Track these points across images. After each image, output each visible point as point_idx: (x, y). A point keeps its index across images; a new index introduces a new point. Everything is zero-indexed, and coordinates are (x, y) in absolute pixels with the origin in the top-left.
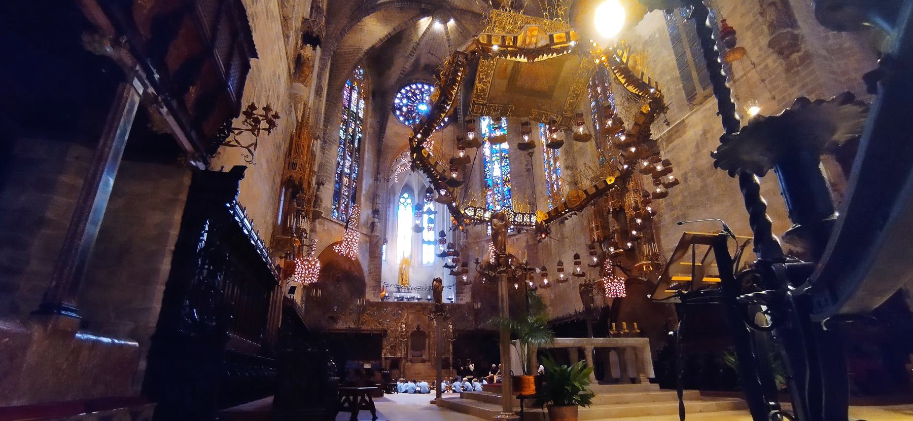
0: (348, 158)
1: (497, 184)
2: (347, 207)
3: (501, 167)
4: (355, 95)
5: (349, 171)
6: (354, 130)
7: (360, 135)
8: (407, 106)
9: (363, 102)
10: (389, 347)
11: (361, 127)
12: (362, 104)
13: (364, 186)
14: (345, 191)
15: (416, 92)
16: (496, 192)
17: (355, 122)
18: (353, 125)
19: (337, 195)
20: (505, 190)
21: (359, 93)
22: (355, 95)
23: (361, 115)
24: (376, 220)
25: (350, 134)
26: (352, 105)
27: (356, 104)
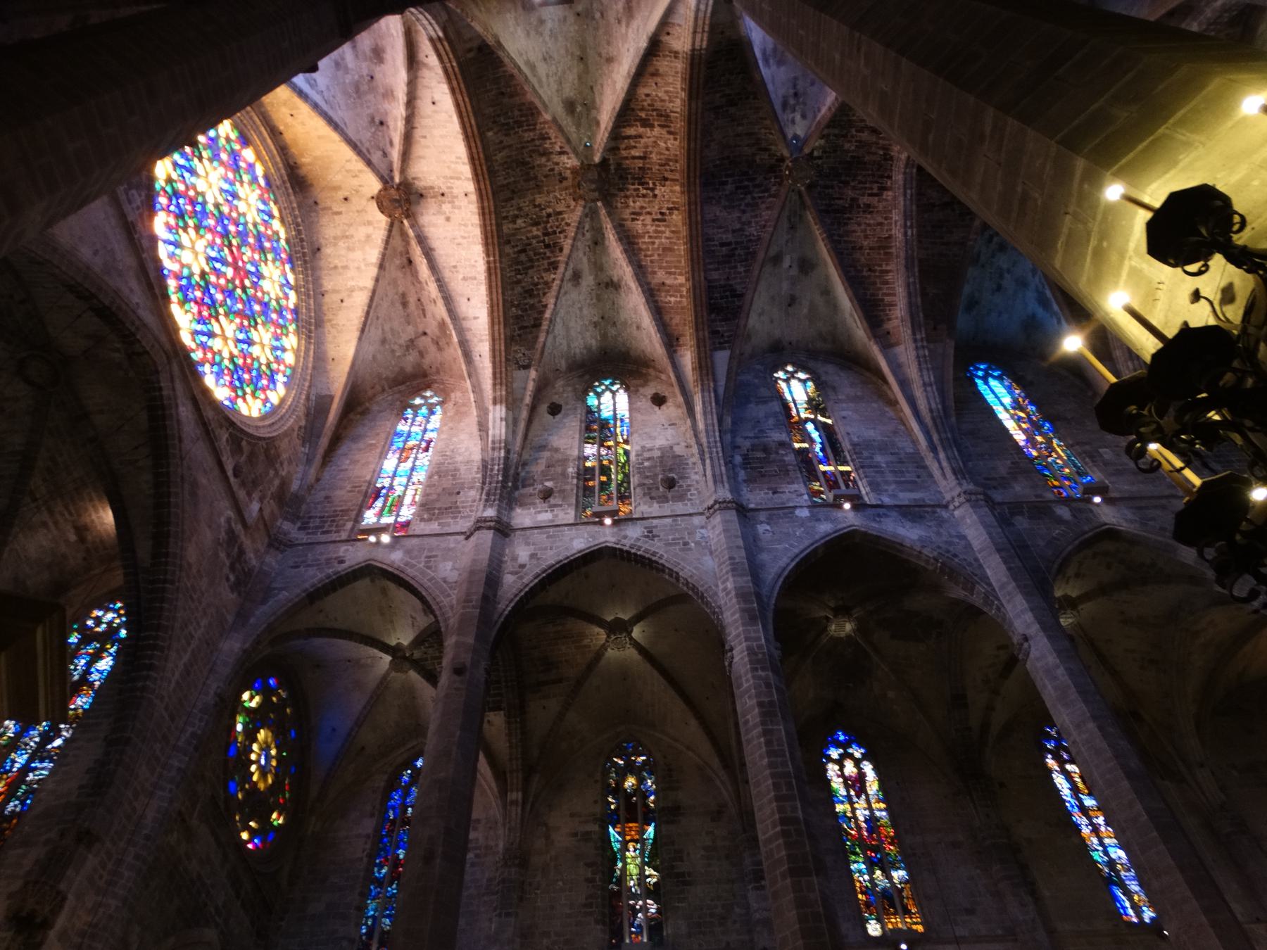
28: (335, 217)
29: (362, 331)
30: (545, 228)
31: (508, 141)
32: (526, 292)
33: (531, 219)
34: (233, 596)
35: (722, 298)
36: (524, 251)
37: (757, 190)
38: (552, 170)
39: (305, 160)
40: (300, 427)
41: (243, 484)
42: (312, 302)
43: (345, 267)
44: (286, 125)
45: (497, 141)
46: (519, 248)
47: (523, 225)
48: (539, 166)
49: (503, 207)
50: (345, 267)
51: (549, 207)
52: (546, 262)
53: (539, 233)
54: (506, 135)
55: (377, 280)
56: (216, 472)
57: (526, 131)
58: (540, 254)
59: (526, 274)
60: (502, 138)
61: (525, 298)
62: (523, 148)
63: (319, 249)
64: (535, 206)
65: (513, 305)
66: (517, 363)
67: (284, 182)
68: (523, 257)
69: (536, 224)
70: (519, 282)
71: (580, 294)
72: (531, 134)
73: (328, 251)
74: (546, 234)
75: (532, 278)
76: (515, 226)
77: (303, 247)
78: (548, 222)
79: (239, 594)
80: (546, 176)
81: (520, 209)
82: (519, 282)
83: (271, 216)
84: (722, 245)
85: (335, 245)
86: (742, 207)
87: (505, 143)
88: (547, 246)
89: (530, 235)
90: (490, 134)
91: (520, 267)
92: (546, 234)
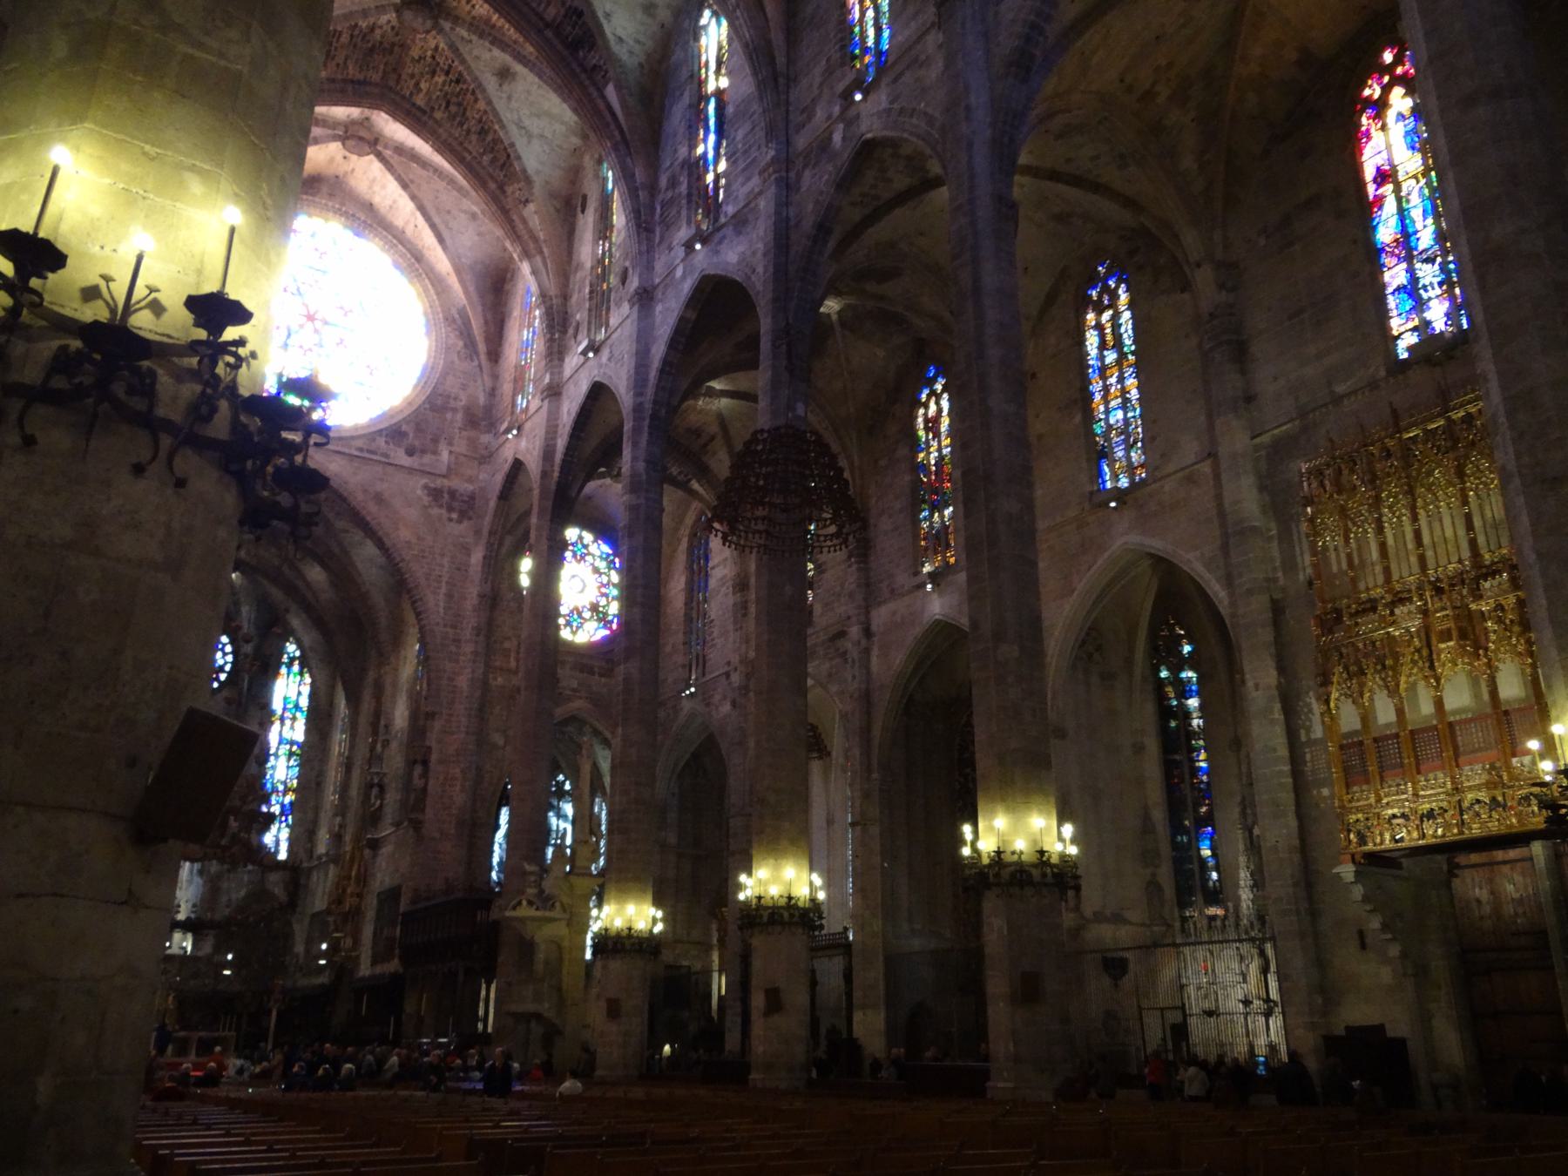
1: (278, 792)
28: (355, 174)
29: (441, 240)
30: (442, 70)
31: (340, 59)
32: (480, 133)
33: (427, 73)
34: (466, 523)
35: (574, 28)
36: (448, 103)
38: (393, 28)
40: (459, 352)
41: (423, 452)
42: (400, 246)
43: (394, 202)
45: (335, 68)
46: (444, 105)
48: (382, 36)
49: (401, 90)
50: (394, 202)
51: (426, 51)
52: (469, 95)
54: (333, 59)
55: (413, 198)
56: (390, 469)
57: (338, 41)
58: (459, 93)
59: (467, 119)
60: (334, 63)
61: (484, 140)
62: (355, 46)
63: (371, 204)
64: (418, 61)
65: (484, 154)
66: (521, 202)
68: (453, 109)
69: (433, 73)
70: (468, 132)
71: (525, 80)
73: (377, 200)
74: (447, 73)
76: (424, 91)
79: (470, 519)
80: (397, 34)
81: (412, 76)
82: (468, 132)
85: (374, 193)
87: (341, 62)
88: (458, 81)
89: (439, 87)
91: (458, 119)
92: (447, 73)
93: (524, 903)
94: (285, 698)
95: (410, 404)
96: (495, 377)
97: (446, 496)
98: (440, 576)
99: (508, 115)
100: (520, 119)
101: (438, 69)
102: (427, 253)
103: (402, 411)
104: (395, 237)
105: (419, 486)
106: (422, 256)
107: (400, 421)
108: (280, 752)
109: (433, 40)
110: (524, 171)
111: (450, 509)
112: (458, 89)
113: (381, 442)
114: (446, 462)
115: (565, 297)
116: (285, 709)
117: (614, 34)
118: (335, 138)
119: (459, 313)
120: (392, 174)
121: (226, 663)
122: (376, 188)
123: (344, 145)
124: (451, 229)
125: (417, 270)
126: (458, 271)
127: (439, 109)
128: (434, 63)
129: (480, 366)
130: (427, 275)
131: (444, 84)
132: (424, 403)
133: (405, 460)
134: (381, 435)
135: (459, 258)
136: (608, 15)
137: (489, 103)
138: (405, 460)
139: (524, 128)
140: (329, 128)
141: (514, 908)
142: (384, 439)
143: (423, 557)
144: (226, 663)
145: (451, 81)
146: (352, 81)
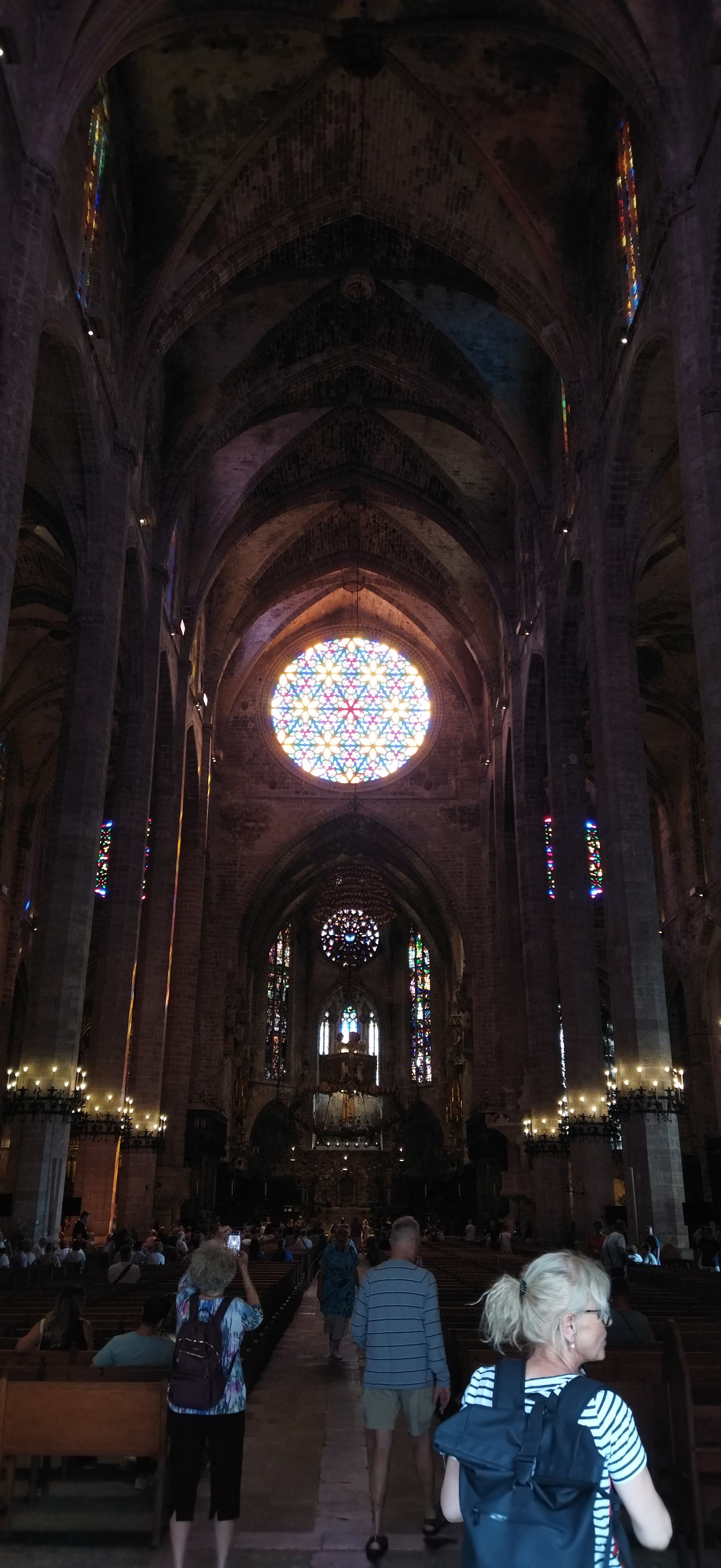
0: (277, 1016)
2: (278, 1065)
3: (424, 1011)
4: (280, 946)
5: (278, 1029)
6: (281, 984)
7: (287, 986)
8: (332, 937)
9: (289, 948)
10: (320, 1193)
11: (288, 977)
12: (288, 953)
13: (293, 1040)
14: (276, 1050)
15: (343, 920)
16: (419, 1037)
17: (282, 974)
18: (280, 979)
19: (269, 1056)
20: (427, 1036)
21: (284, 943)
22: (280, 946)
23: (287, 965)
24: (306, 1072)
25: (277, 991)
26: (278, 959)
27: (281, 956)
29: (424, 629)
33: (374, 533)
37: (369, 425)
39: (323, 611)
42: (401, 639)
44: (299, 624)
46: (391, 549)
47: (377, 539)
48: (340, 521)
51: (369, 520)
53: (385, 532)
54: (314, 547)
55: (399, 607)
63: (377, 616)
67: (332, 628)
68: (397, 549)
69: (378, 531)
72: (316, 531)
73: (379, 612)
74: (386, 529)
75: (411, 551)
76: (377, 543)
77: (371, 629)
78: (379, 524)
80: (348, 516)
81: (366, 537)
83: (345, 649)
84: (403, 464)
85: (377, 608)
86: (380, 439)
90: (311, 558)
92: (386, 529)
93: (501, 1116)
94: (416, 959)
95: (424, 752)
96: (481, 716)
97: (457, 813)
98: (461, 873)
99: (432, 543)
100: (441, 541)
101: (380, 528)
102: (419, 638)
103: (419, 758)
104: (397, 633)
105: (438, 810)
106: (418, 641)
107: (418, 766)
108: (418, 1000)
109: (371, 513)
110: (451, 577)
111: (462, 822)
112: (396, 536)
113: (407, 785)
114: (454, 788)
115: (497, 659)
116: (416, 967)
117: (465, 483)
118: (338, 587)
119: (449, 675)
120: (381, 596)
121: (375, 938)
122: (377, 605)
123: (344, 588)
124: (430, 618)
125: (416, 652)
126: (440, 647)
127: (389, 552)
128: (376, 525)
129: (469, 709)
130: (423, 654)
131: (386, 534)
132: (433, 748)
133: (427, 795)
134: (407, 780)
135: (440, 637)
136: (457, 473)
137: (416, 539)
138: (427, 795)
139: (445, 547)
140: (331, 583)
141: (495, 1121)
142: (409, 782)
143: (448, 861)
144: (375, 938)
145: (390, 532)
146: (330, 555)
